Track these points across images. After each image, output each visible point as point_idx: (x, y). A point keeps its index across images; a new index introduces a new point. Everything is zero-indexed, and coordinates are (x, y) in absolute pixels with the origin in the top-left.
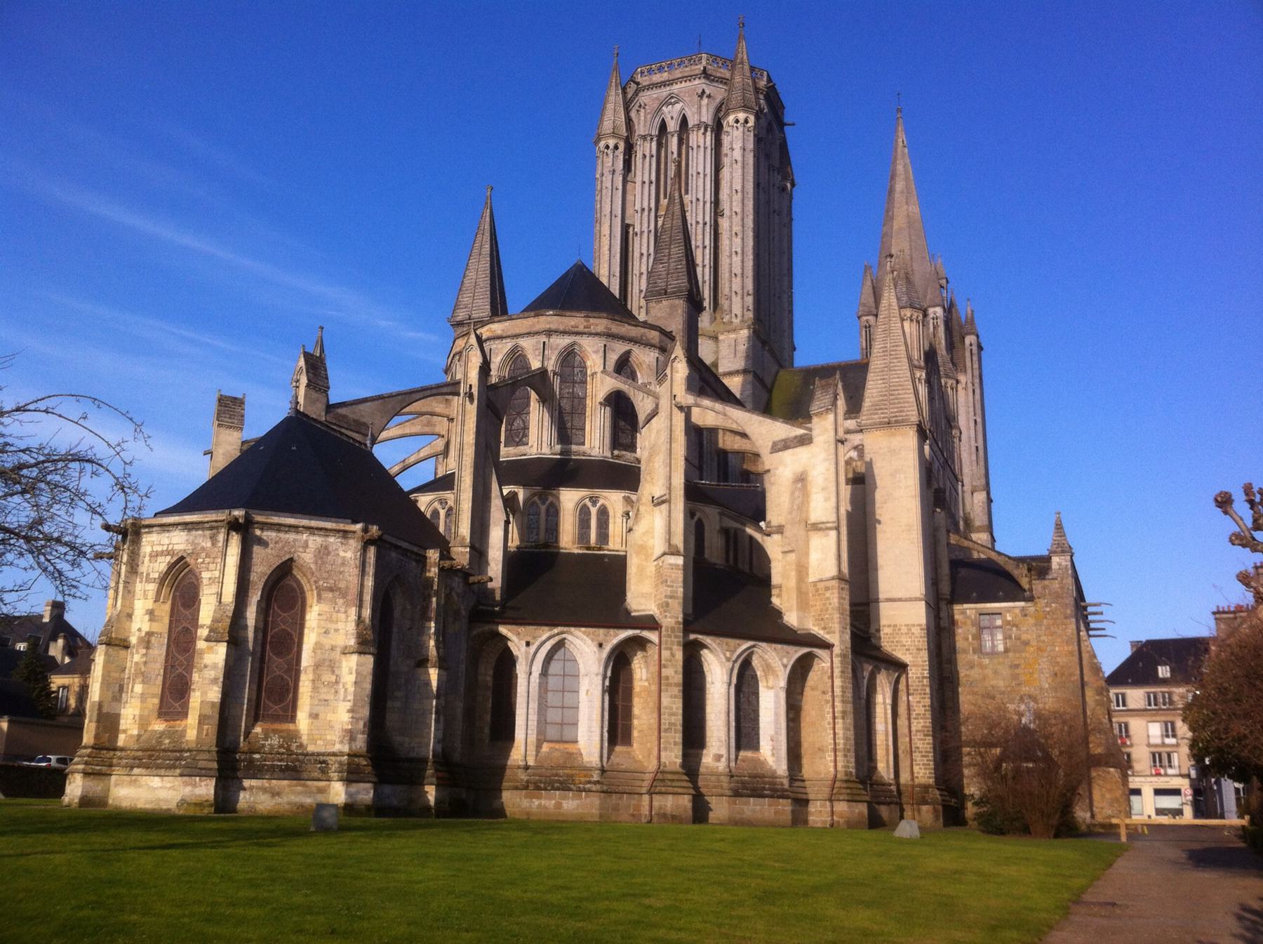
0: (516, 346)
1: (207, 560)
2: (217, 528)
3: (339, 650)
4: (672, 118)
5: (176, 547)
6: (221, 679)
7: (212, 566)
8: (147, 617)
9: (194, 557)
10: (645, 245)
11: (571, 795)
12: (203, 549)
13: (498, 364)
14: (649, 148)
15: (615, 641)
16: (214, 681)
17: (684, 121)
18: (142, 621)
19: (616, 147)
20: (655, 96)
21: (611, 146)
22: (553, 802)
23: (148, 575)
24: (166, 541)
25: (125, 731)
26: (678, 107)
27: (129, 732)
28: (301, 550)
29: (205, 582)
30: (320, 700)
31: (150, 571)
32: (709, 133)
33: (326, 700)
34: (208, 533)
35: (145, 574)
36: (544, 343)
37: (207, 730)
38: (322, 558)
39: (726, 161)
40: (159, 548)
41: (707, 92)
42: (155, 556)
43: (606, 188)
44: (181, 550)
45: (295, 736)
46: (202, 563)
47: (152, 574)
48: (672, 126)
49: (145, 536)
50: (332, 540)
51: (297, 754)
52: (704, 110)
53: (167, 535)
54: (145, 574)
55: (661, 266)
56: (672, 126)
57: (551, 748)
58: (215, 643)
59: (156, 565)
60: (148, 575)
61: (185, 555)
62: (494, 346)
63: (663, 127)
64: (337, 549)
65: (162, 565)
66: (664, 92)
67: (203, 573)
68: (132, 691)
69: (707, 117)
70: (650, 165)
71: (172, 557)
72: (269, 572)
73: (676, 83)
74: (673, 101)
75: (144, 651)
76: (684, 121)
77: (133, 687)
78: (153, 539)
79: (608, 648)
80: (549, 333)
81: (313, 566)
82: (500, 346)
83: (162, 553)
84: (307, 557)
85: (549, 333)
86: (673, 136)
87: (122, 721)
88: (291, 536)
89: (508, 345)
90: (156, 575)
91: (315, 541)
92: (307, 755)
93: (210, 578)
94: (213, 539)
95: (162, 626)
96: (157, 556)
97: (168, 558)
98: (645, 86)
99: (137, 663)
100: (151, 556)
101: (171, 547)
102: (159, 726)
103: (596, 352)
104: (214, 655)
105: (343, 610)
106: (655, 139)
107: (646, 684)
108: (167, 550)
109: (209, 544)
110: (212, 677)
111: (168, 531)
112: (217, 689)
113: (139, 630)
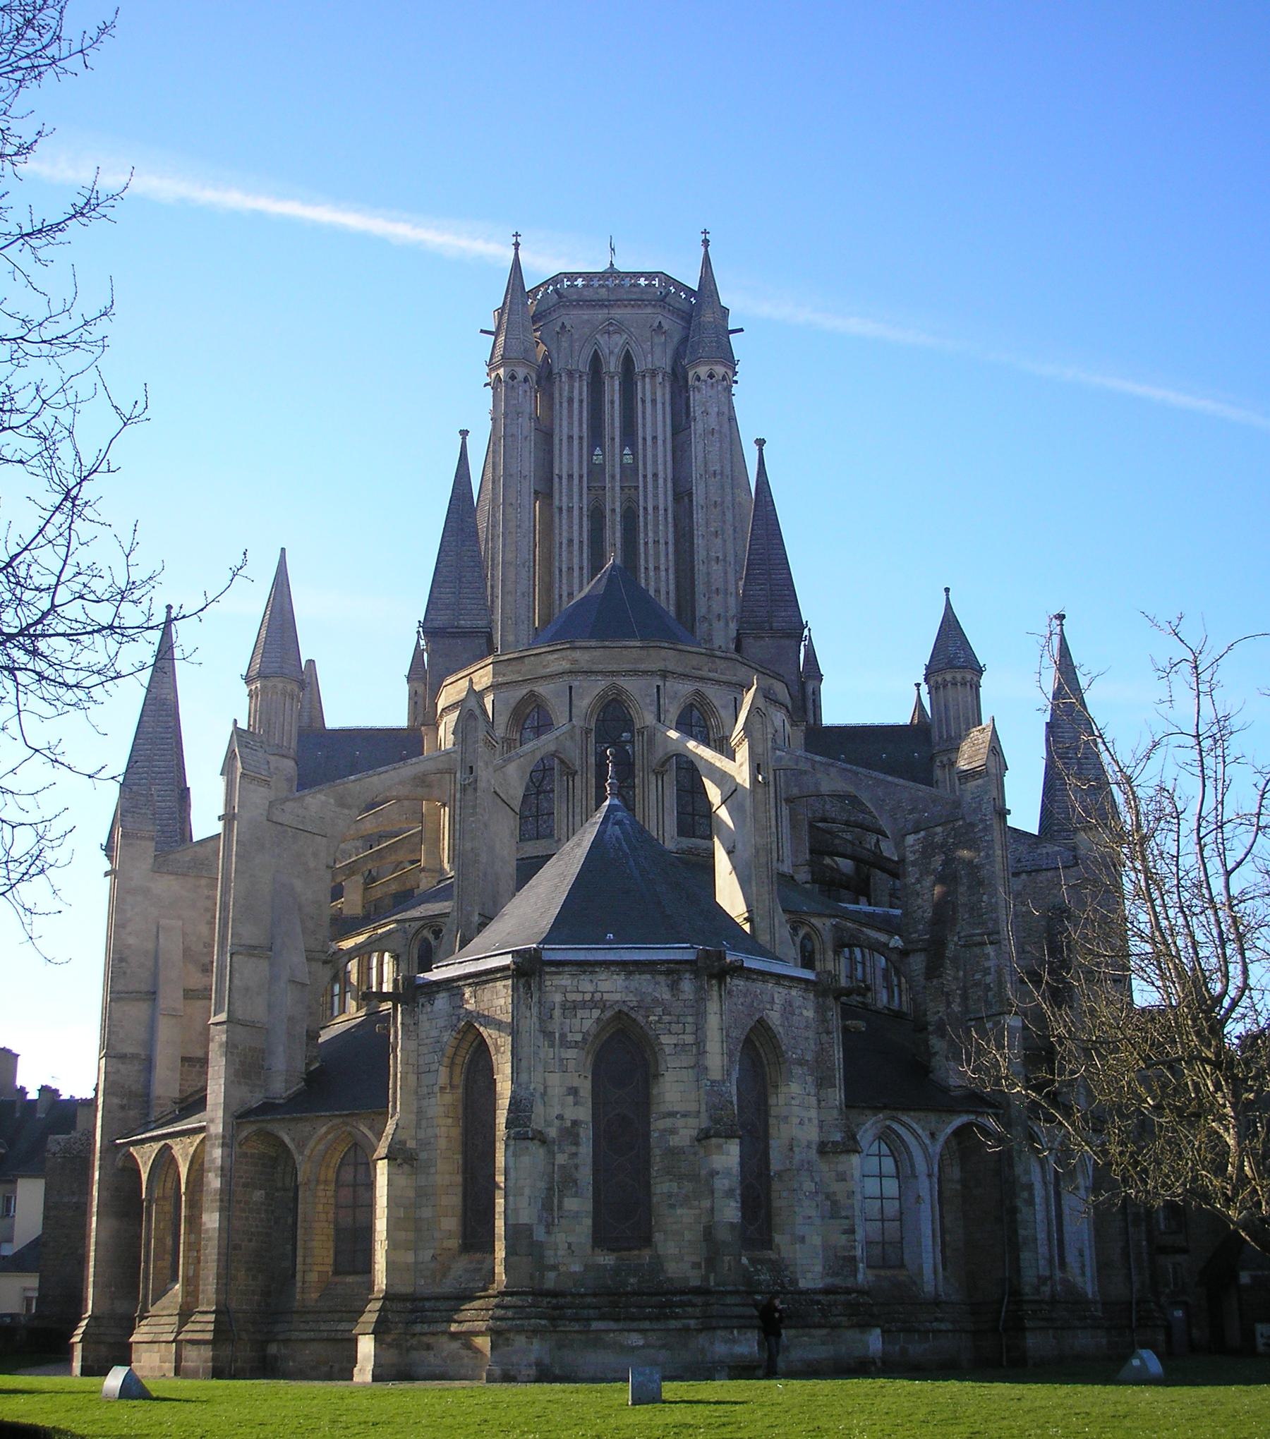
0: (614, 686)
1: (666, 1018)
2: (677, 972)
3: (814, 1147)
4: (611, 353)
5: (606, 996)
6: (738, 1192)
7: (674, 1028)
8: (570, 1099)
9: (642, 1012)
10: (576, 527)
11: (916, 1337)
12: (655, 1000)
13: (584, 711)
14: (581, 390)
15: (949, 1130)
16: (729, 1193)
17: (628, 361)
18: (563, 1105)
19: (526, 380)
20: (586, 317)
21: (520, 377)
22: (897, 1348)
23: (563, 1036)
24: (590, 988)
25: (554, 1268)
26: (619, 340)
27: (563, 1269)
28: (768, 1006)
29: (667, 1050)
30: (804, 1217)
31: (567, 1029)
32: (668, 385)
33: (810, 1217)
34: (661, 978)
35: (557, 1035)
36: (658, 687)
37: (729, 1262)
38: (787, 1019)
39: (698, 427)
40: (579, 997)
41: (666, 327)
42: (571, 1008)
43: (512, 435)
44: (618, 1001)
45: (777, 1267)
46: (659, 1022)
47: (569, 1034)
48: (612, 365)
49: (547, 977)
50: (794, 992)
51: (792, 1293)
52: (658, 350)
53: (590, 977)
54: (557, 1035)
55: (758, 587)
56: (612, 365)
57: (877, 1276)
58: (724, 1140)
59: (577, 1021)
60: (563, 1036)
61: (625, 1009)
62: (577, 683)
63: (596, 361)
64: (799, 1007)
65: (587, 1021)
66: (601, 314)
67: (661, 1037)
68: (560, 1208)
69: (663, 361)
70: (581, 413)
71: (602, 1012)
72: (743, 1037)
73: (619, 307)
74: (611, 329)
75: (574, 1149)
76: (628, 361)
77: (560, 1202)
78: (564, 982)
79: (941, 1139)
80: (664, 674)
81: (781, 1029)
82: (585, 684)
83: (584, 1005)
84: (775, 1018)
85: (664, 674)
86: (613, 377)
87: (549, 1253)
88: (758, 986)
89: (601, 684)
90: (579, 1037)
91: (780, 994)
92: (801, 1293)
93: (675, 1045)
94: (674, 987)
95: (584, 1113)
96: (575, 1008)
97: (596, 1013)
98: (571, 302)
99: (562, 1167)
100: (564, 1007)
101: (597, 997)
102: (607, 1259)
103: (724, 707)
104: (724, 1157)
105: (813, 1092)
106: (585, 377)
107: (959, 1187)
108: (592, 1000)
109: (667, 996)
110: (726, 1187)
111: (592, 973)
112: (733, 1204)
113: (560, 1117)
